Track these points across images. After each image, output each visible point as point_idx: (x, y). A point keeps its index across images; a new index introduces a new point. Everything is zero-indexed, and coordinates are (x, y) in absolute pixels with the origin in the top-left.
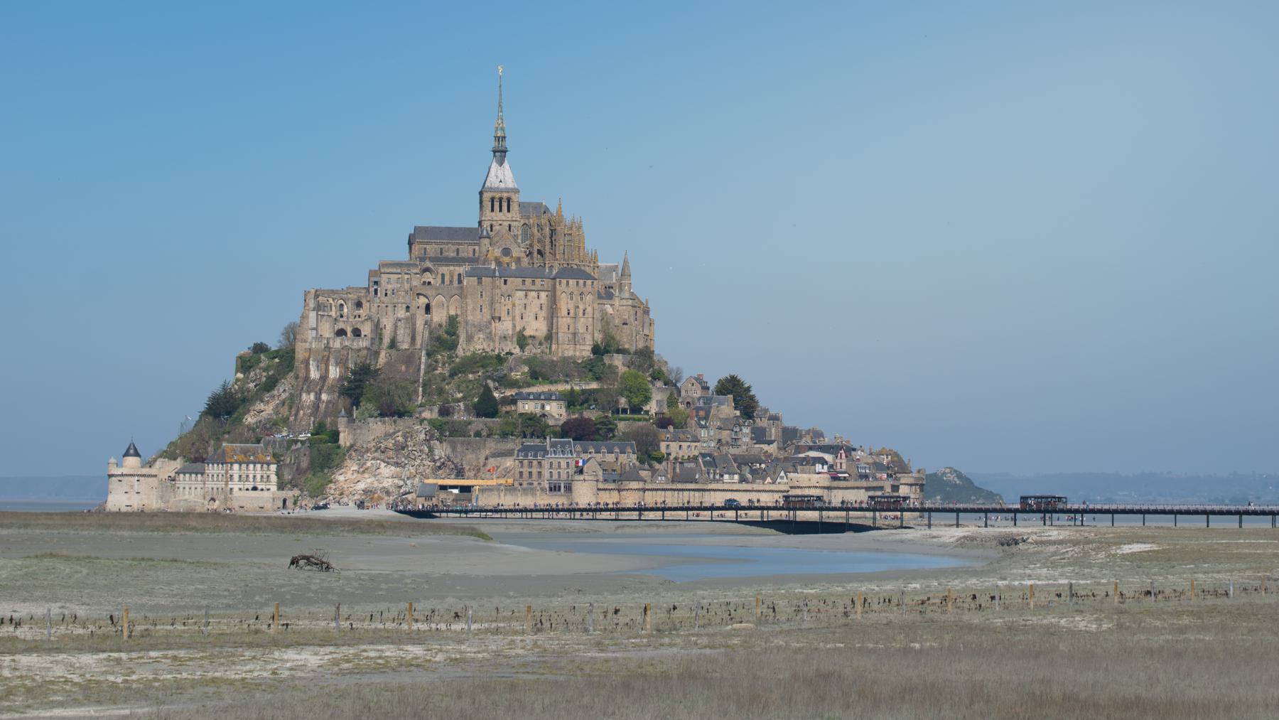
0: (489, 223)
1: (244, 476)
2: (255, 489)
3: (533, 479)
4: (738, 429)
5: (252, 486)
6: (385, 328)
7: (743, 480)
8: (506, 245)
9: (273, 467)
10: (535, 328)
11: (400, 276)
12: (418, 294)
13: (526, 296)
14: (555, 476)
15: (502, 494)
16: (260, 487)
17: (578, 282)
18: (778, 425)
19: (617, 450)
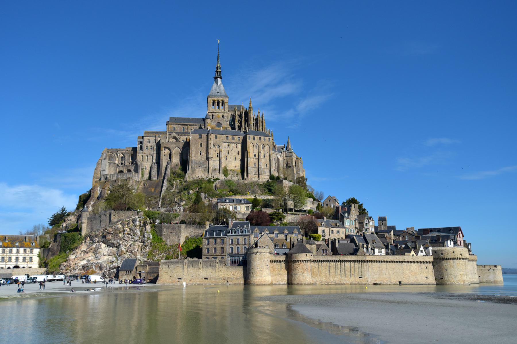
0: (211, 114)
1: (7, 258)
2: (17, 267)
3: (218, 254)
4: (367, 222)
5: (14, 265)
6: (146, 168)
7: (387, 254)
8: (219, 121)
9: (36, 251)
10: (234, 165)
11: (155, 138)
12: (165, 148)
13: (229, 146)
14: (235, 251)
15: (186, 266)
16: (21, 266)
17: (260, 138)
18: (386, 224)
19: (286, 232)
